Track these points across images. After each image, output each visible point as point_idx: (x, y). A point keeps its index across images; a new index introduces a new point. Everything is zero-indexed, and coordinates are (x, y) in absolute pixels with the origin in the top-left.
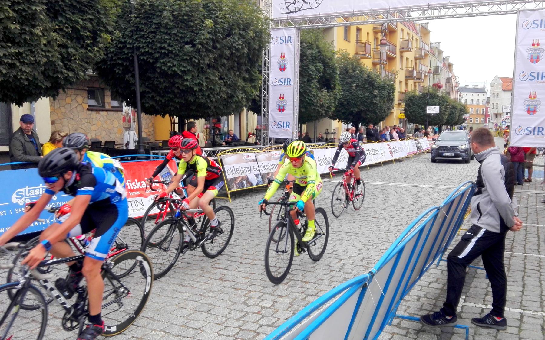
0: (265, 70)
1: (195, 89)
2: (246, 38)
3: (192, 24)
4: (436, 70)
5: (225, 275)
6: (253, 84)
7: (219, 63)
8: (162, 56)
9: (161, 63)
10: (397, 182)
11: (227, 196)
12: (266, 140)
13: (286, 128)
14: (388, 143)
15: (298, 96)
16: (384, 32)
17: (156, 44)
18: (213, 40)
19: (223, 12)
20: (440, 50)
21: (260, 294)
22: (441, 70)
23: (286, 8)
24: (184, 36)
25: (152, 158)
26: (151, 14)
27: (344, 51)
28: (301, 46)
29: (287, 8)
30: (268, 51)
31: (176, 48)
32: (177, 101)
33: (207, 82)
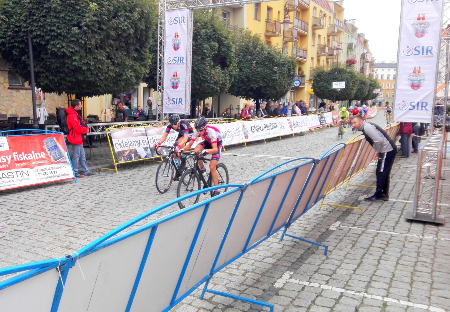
0: (160, 50)
1: (83, 69)
2: (132, 19)
3: (78, 7)
5: (73, 243)
6: (142, 63)
8: (53, 38)
9: (51, 44)
10: (287, 156)
11: (114, 168)
12: (161, 115)
13: (179, 104)
14: (287, 118)
15: (191, 73)
17: (46, 27)
18: (98, 22)
22: (355, 47)
31: (64, 31)
32: (68, 80)
33: (95, 62)
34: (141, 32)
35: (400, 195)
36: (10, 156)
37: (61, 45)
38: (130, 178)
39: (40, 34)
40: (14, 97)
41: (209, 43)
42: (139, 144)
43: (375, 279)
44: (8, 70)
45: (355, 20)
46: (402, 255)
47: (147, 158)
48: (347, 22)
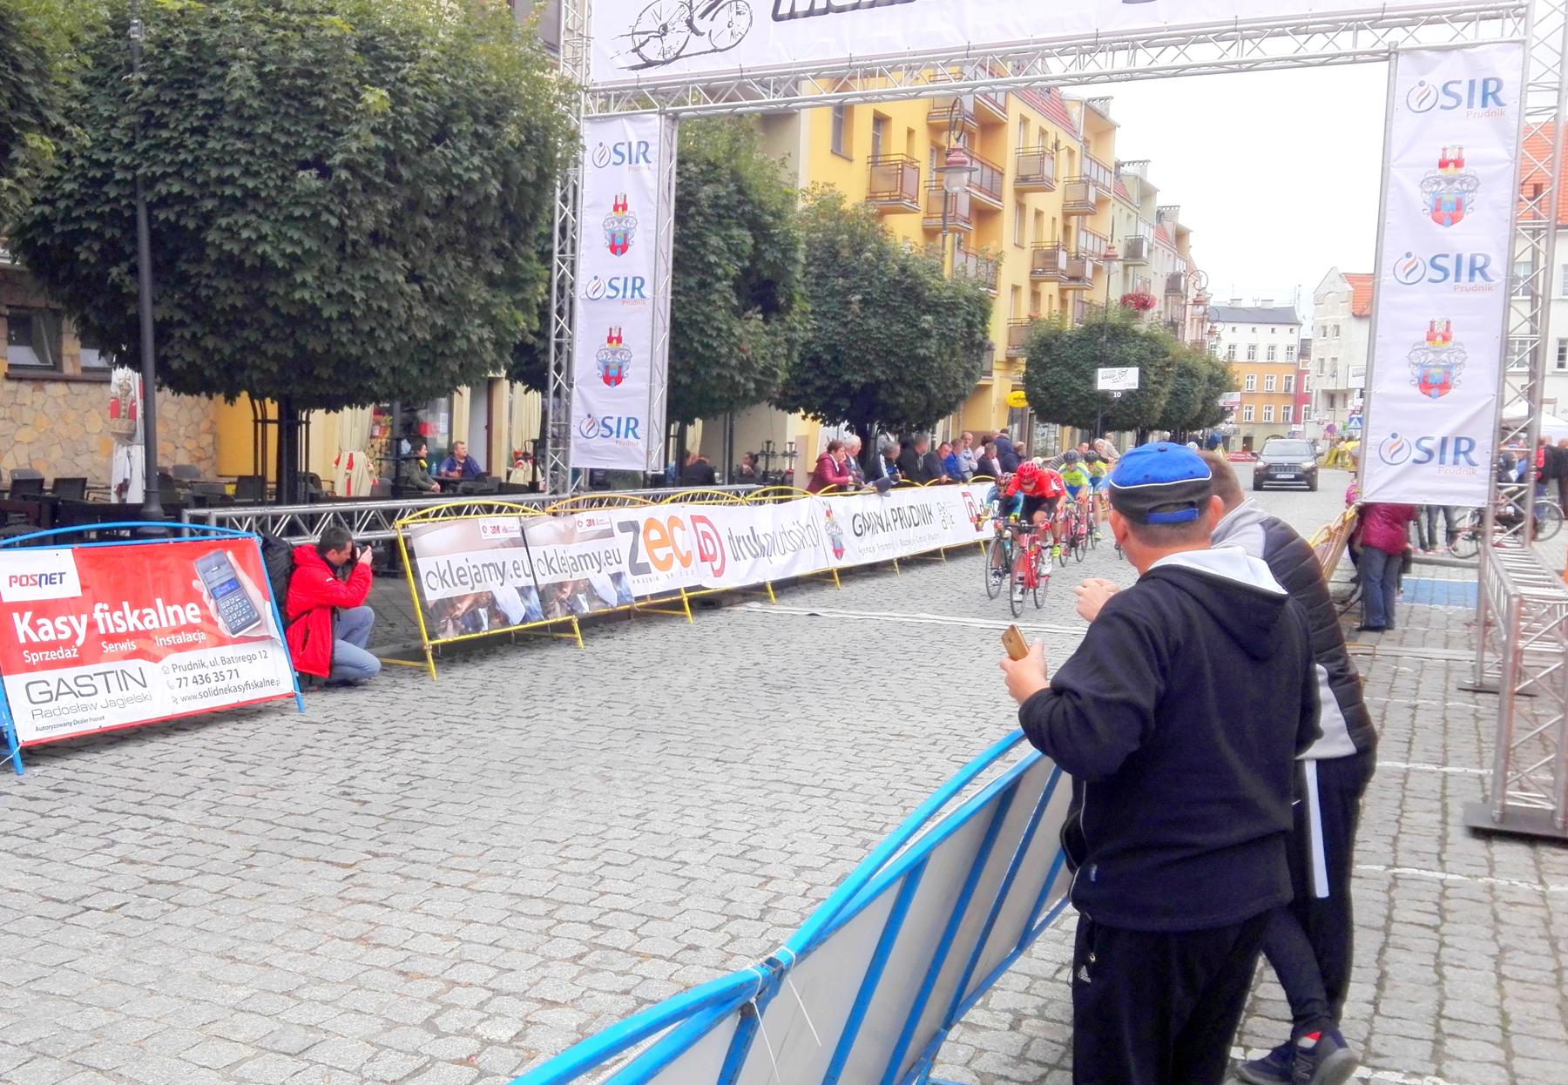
0: (562, 252)
1: (326, 314)
2: (497, 147)
3: (321, 103)
4: (1134, 251)
6: (519, 297)
7: (408, 230)
9: (220, 226)
13: (626, 436)
14: (962, 487)
15: (667, 334)
16: (959, 125)
17: (205, 168)
18: (386, 153)
19: (422, 65)
20: (1148, 184)
21: (486, 994)
22: (1149, 251)
23: (633, 51)
24: (297, 144)
25: (186, 532)
26: (193, 71)
27: (827, 189)
28: (679, 174)
29: (636, 50)
30: (575, 187)
32: (270, 353)
34: (520, 192)
35: (1413, 747)
36: (84, 618)
37: (257, 230)
38: (484, 692)
39: (181, 192)
40: (24, 408)
41: (723, 233)
42: (503, 576)
43: (1451, 1031)
44: (7, 312)
45: (1148, 161)
46: (1502, 950)
47: (529, 625)
48: (1123, 170)
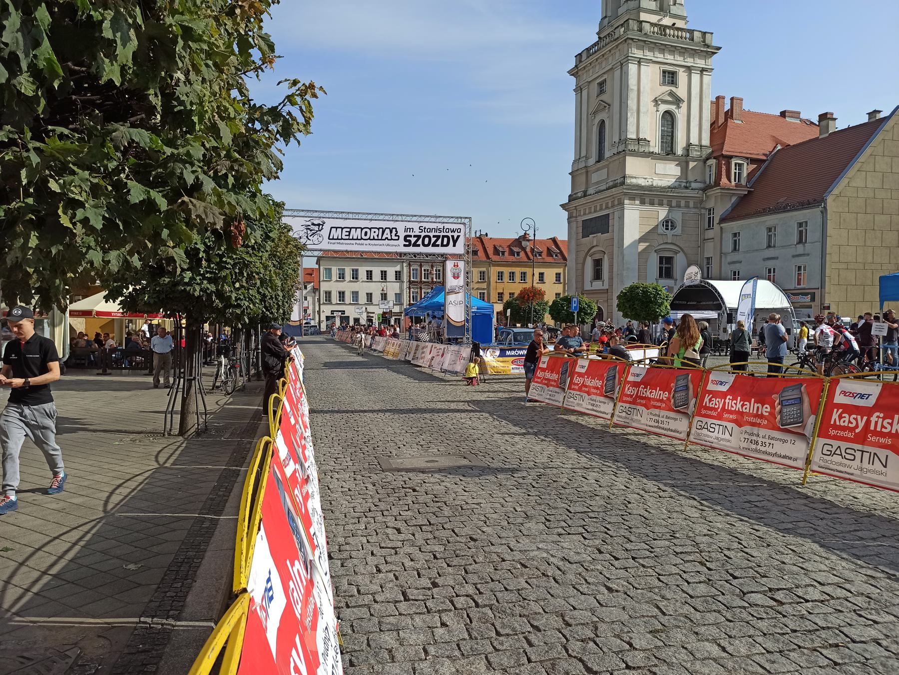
36: (865, 418)
